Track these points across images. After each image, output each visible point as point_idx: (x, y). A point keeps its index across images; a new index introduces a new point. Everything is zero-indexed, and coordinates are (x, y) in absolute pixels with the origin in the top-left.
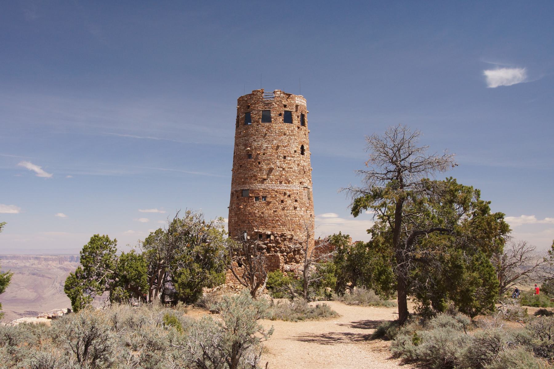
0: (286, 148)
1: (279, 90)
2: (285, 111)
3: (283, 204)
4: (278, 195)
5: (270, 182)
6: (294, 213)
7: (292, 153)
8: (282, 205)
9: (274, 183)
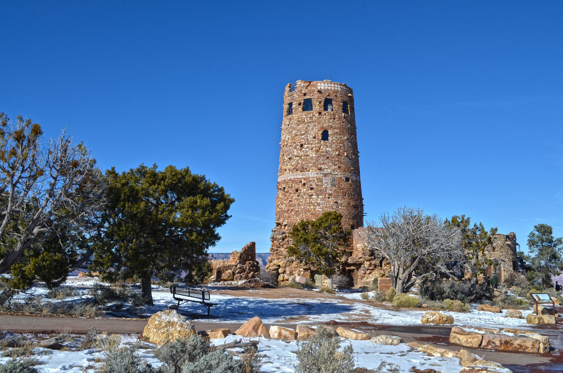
1: (300, 81)
2: (304, 100)
3: (297, 193)
4: (293, 185)
5: (288, 173)
6: (308, 202)
7: (309, 140)
9: (291, 172)
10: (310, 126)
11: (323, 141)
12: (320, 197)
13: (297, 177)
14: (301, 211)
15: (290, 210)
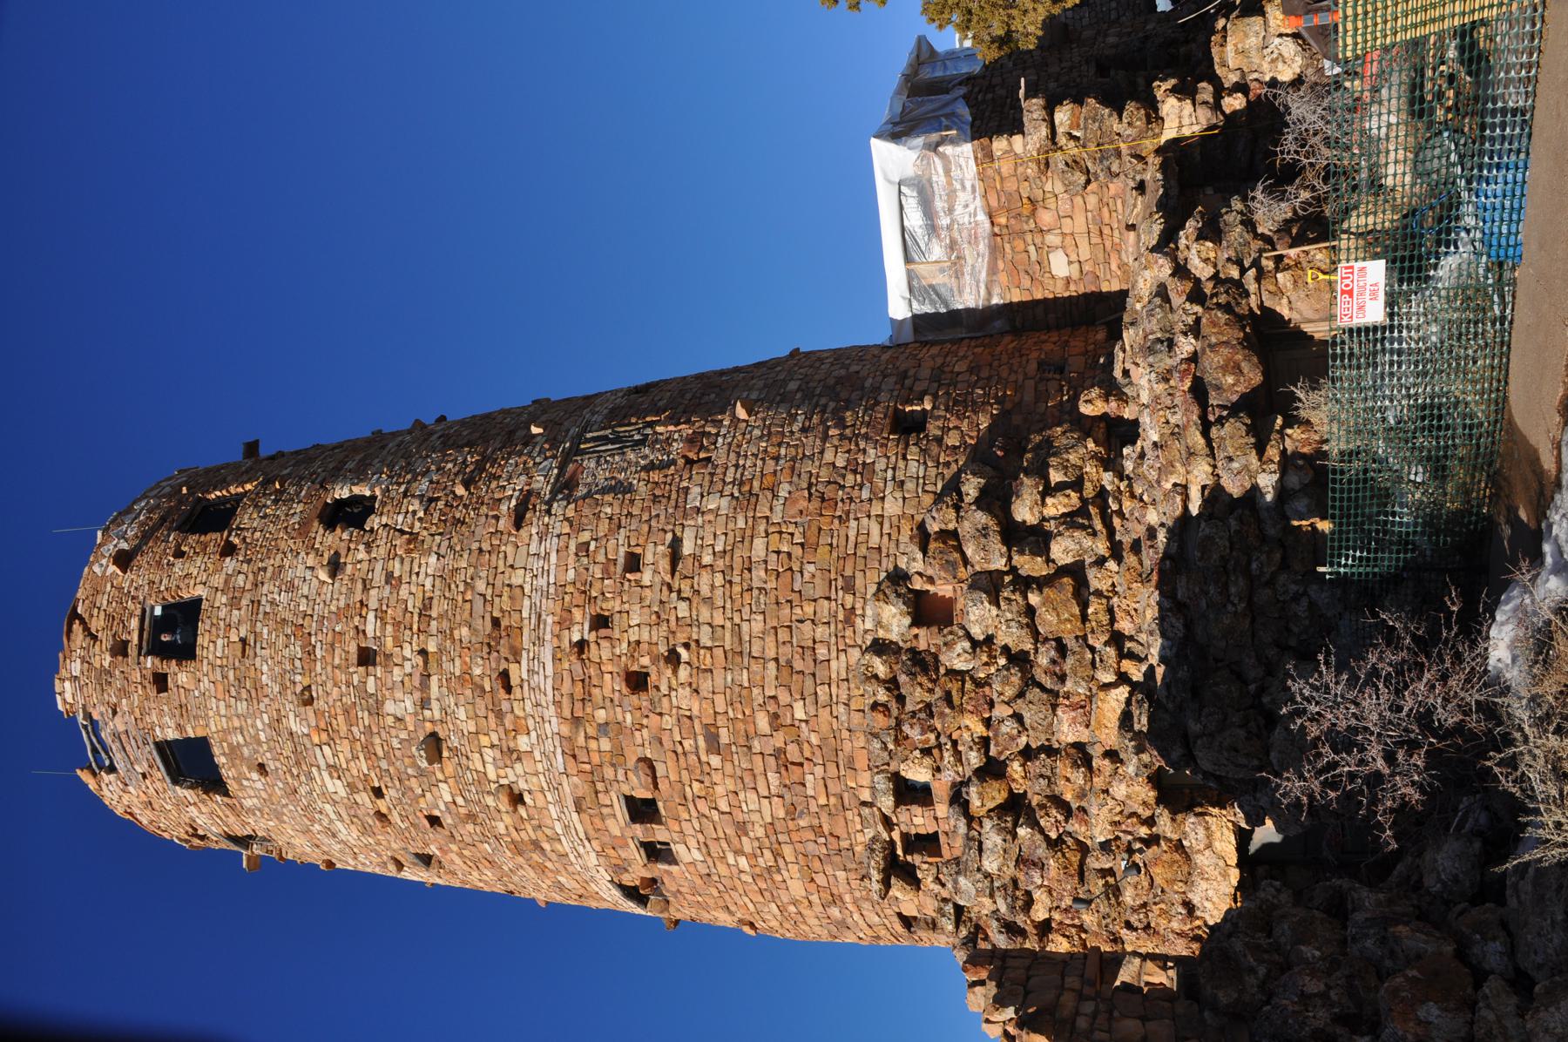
0: (319, 653)
1: (57, 682)
4: (601, 715)
5: (527, 765)
6: (719, 579)
7: (342, 604)
8: (664, 689)
9: (523, 743)
10: (272, 603)
11: (373, 516)
12: (693, 500)
13: (550, 682)
14: (783, 635)
15: (779, 740)
